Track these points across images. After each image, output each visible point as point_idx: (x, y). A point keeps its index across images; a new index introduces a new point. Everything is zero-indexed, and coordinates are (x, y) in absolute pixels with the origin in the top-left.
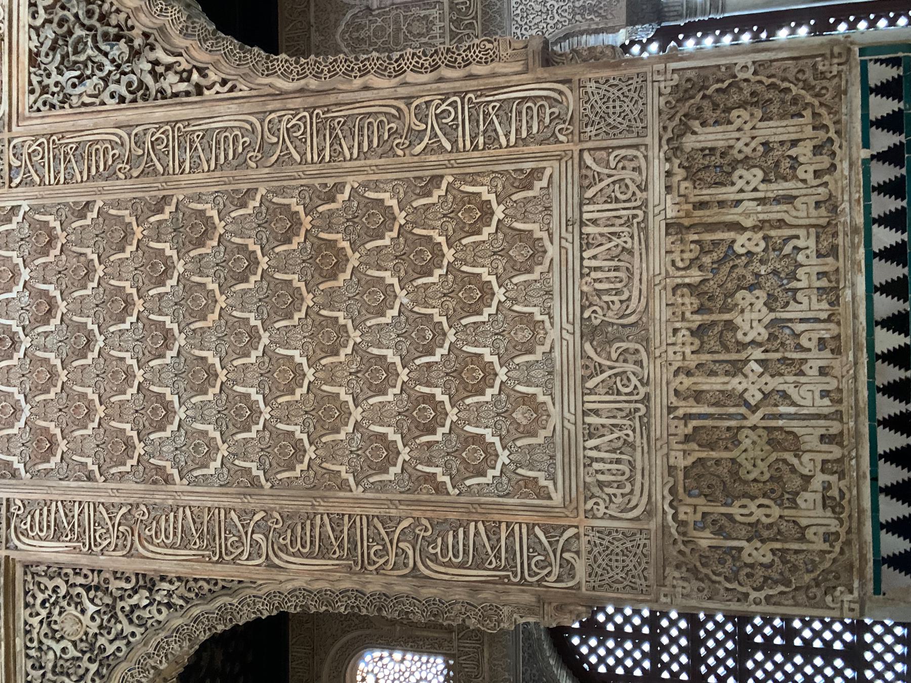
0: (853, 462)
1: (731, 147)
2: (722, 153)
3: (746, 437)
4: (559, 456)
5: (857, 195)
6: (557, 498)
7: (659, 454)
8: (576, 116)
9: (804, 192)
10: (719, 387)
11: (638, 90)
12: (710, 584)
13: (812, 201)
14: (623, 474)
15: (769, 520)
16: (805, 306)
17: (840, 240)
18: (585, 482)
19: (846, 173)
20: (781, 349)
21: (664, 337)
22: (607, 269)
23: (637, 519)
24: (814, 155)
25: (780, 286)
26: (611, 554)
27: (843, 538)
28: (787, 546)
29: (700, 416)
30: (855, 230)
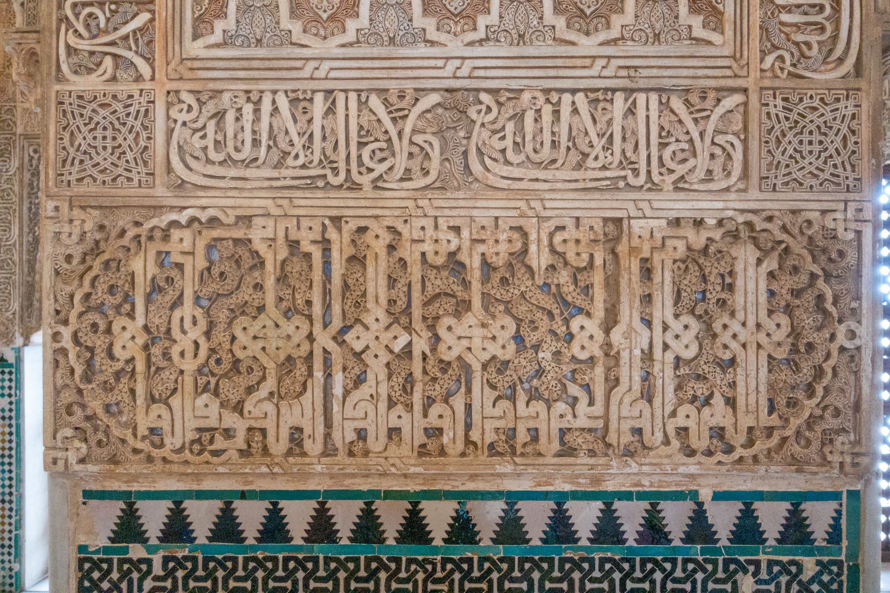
0: (264, 469)
1: (733, 314)
2: (724, 302)
3: (298, 328)
4: (261, 52)
5: (647, 483)
6: (195, 48)
7: (269, 203)
8: (801, 83)
9: (658, 413)
10: (371, 291)
11: (835, 180)
12: (79, 273)
13: (645, 424)
14: (237, 150)
15: (176, 357)
16: (489, 411)
17: (584, 459)
18: (221, 92)
19: (681, 470)
20: (428, 378)
21: (447, 212)
22: (556, 129)
23: (169, 169)
24: (711, 429)
25: (519, 378)
26: (114, 129)
27: (156, 453)
28: (140, 378)
29: (327, 264)
30: (596, 480)
